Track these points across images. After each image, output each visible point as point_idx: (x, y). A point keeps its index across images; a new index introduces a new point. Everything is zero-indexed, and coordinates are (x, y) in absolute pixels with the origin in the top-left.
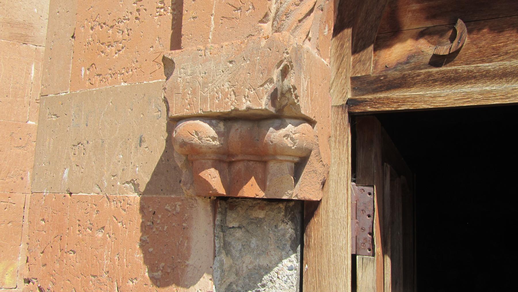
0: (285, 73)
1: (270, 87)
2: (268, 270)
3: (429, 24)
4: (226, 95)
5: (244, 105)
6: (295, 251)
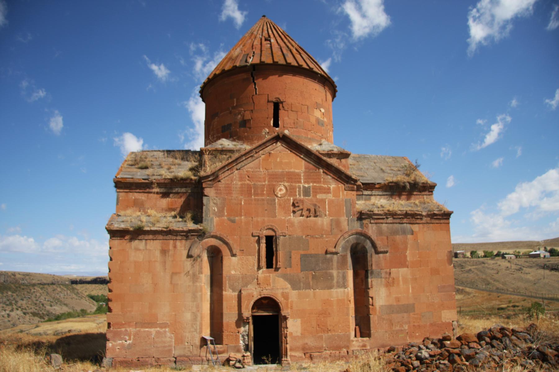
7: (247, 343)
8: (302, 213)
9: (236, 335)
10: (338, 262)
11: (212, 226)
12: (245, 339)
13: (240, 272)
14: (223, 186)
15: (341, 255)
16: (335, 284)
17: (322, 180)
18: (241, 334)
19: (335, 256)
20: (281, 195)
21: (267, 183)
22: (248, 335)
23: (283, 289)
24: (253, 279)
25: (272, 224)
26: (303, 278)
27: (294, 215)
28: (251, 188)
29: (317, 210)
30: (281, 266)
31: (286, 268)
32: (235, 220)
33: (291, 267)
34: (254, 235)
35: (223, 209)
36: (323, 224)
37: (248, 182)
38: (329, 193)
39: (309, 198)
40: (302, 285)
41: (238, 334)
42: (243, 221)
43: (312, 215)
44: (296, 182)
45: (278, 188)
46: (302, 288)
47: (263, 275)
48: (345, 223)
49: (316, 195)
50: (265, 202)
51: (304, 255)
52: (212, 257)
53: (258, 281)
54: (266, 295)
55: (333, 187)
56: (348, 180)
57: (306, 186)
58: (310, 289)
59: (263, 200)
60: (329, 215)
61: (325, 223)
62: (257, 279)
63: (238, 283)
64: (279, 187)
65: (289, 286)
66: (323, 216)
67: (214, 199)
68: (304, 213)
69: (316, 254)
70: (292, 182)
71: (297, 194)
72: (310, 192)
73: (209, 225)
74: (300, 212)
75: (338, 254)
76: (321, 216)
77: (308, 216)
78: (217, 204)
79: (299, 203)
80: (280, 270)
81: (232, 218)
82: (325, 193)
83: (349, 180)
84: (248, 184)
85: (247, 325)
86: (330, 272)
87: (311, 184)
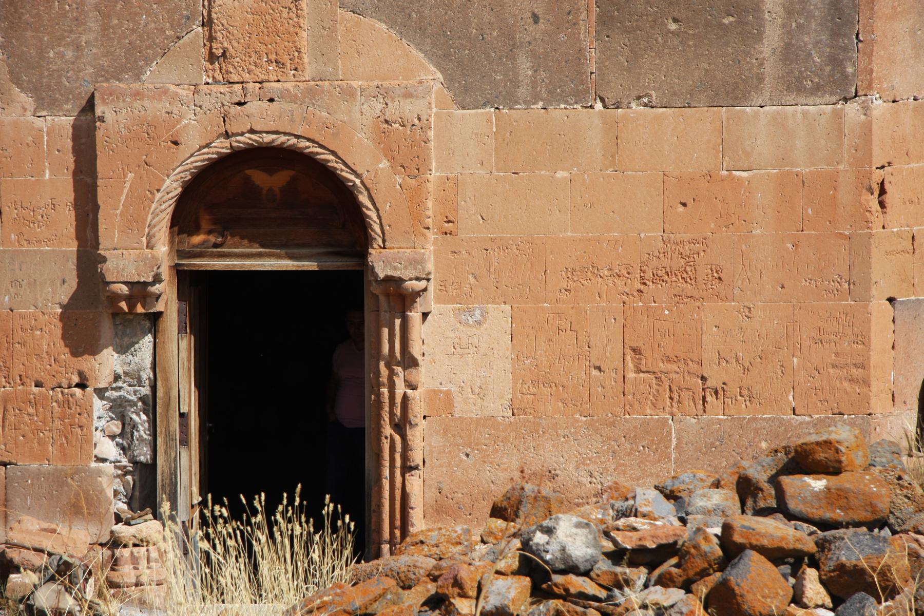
0: (158, 268)
1: (153, 273)
2: (138, 343)
3: (213, 227)
4: (134, 275)
5: (142, 280)
6: (150, 332)
7: (144, 455)
9: (66, 403)
12: (134, 426)
16: (771, 69)
18: (100, 393)
22: (150, 405)
23: (384, 93)
24: (181, 25)
26: (536, 18)
40: (525, 66)
41: (78, 391)
46: (523, 91)
53: (211, 39)
54: (267, 138)
58: (579, 96)
62: (208, 23)
63: (78, 48)
65: (433, 77)
85: (144, 334)
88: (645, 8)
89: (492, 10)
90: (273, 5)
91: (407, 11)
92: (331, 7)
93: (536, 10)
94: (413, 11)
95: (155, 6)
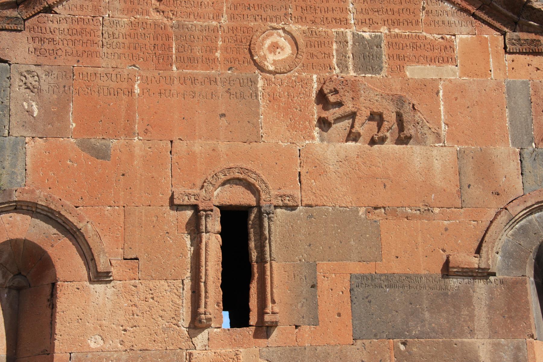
8: (352, 126)
10: (490, 307)
11: (19, 169)
13: (122, 342)
14: (64, 26)
15: (502, 282)
17: (422, 15)
19: (480, 285)
20: (275, 62)
21: (224, 20)
25: (244, 166)
27: (325, 134)
28: (168, 38)
29: (405, 117)
30: (277, 318)
31: (297, 327)
32: (108, 147)
33: (315, 322)
34: (176, 202)
35: (64, 108)
36: (429, 168)
37: (157, 17)
38: (451, 60)
39: (378, 76)
42: (137, 151)
43: (388, 134)
44: (325, 21)
45: (263, 40)
47: (211, 354)
48: (514, 166)
49: (401, 69)
50: (220, 88)
51: (363, 277)
52: (19, 289)
55: (461, 40)
56: (516, 17)
57: (367, 35)
59: (212, 80)
60: (451, 136)
61: (437, 165)
64: (268, 36)
66: (431, 139)
67: (29, 72)
68: (357, 128)
69: (408, 277)
70: (314, 22)
71: (334, 61)
72: (379, 57)
73: (7, 164)
74: (347, 123)
75: (492, 278)
76: (421, 141)
77: (376, 138)
78: (40, 90)
79: (341, 92)
80: (275, 333)
81: (97, 141)
82: (431, 61)
83: (519, 15)
84: (156, 24)
86: (462, 343)
87: (384, 30)
88: (420, 359)
89: (341, 359)
90: (224, 357)
91: (296, 360)
92: (255, 358)
93: (364, 359)
94: (299, 359)
95: (159, 359)
